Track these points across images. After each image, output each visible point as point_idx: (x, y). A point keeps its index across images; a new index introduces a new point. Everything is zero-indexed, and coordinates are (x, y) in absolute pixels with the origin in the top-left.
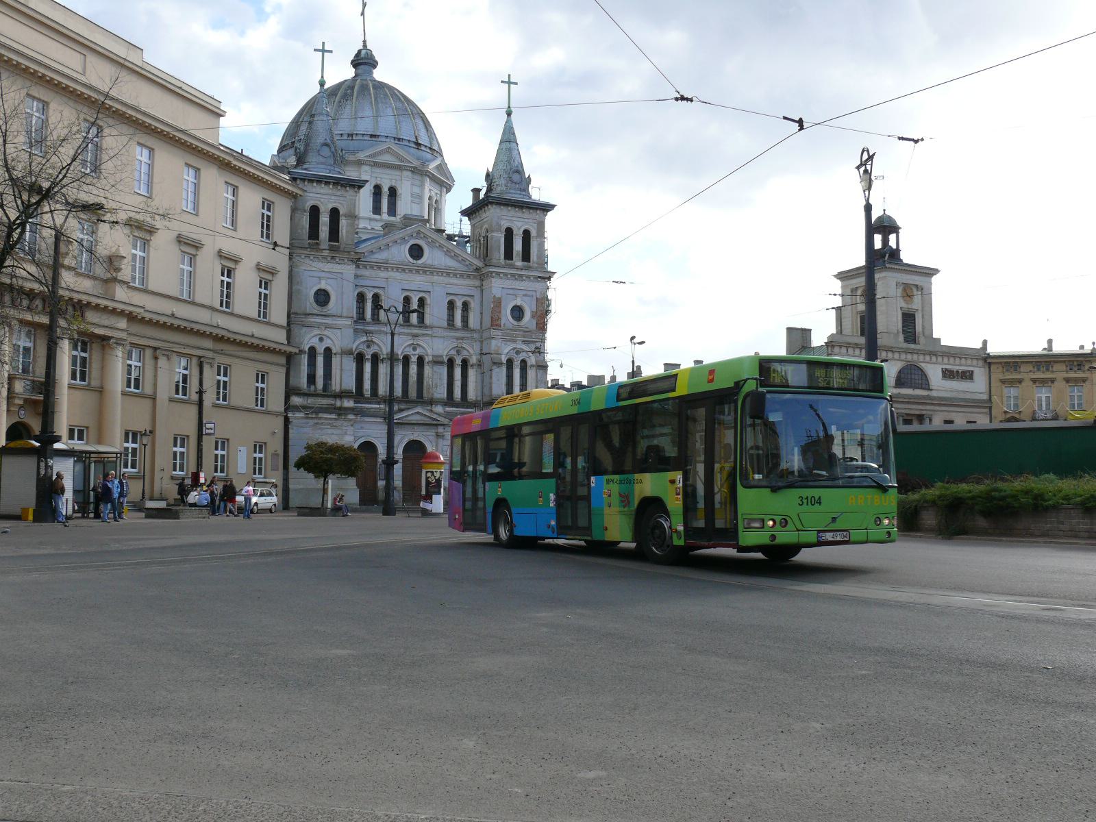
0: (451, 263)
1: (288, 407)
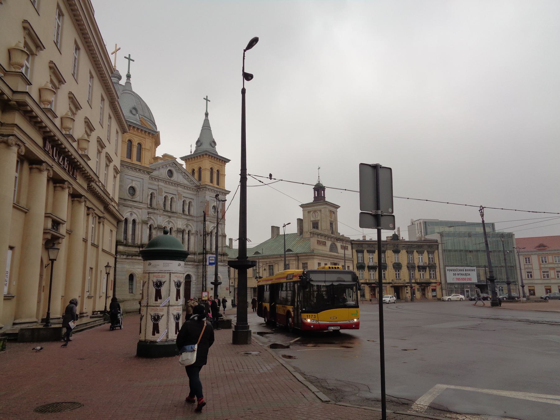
0: (186, 182)
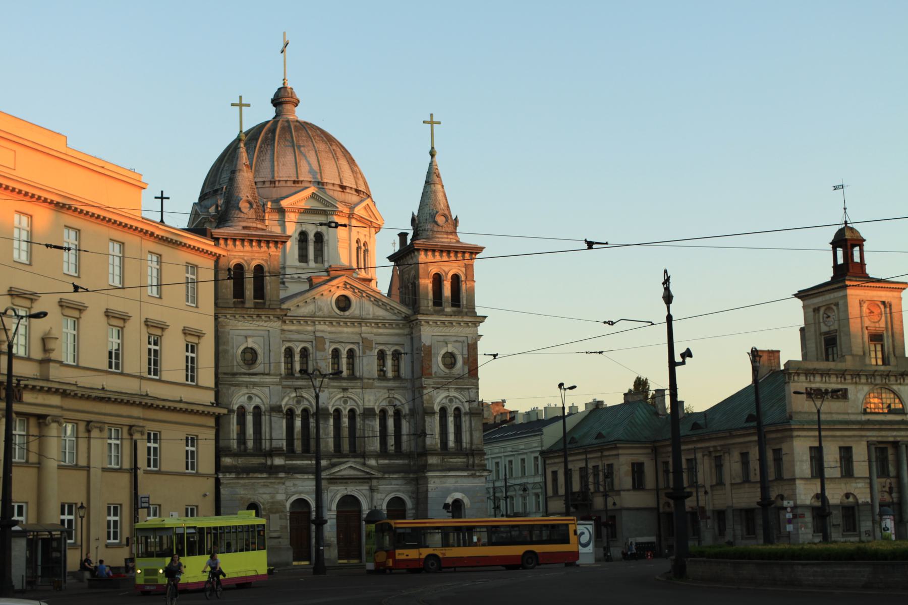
1: (218, 467)
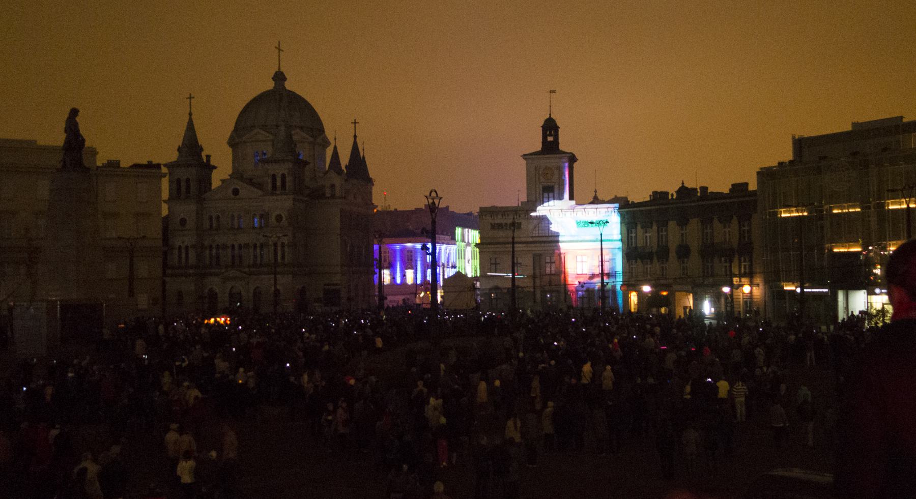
1: (164, 274)
